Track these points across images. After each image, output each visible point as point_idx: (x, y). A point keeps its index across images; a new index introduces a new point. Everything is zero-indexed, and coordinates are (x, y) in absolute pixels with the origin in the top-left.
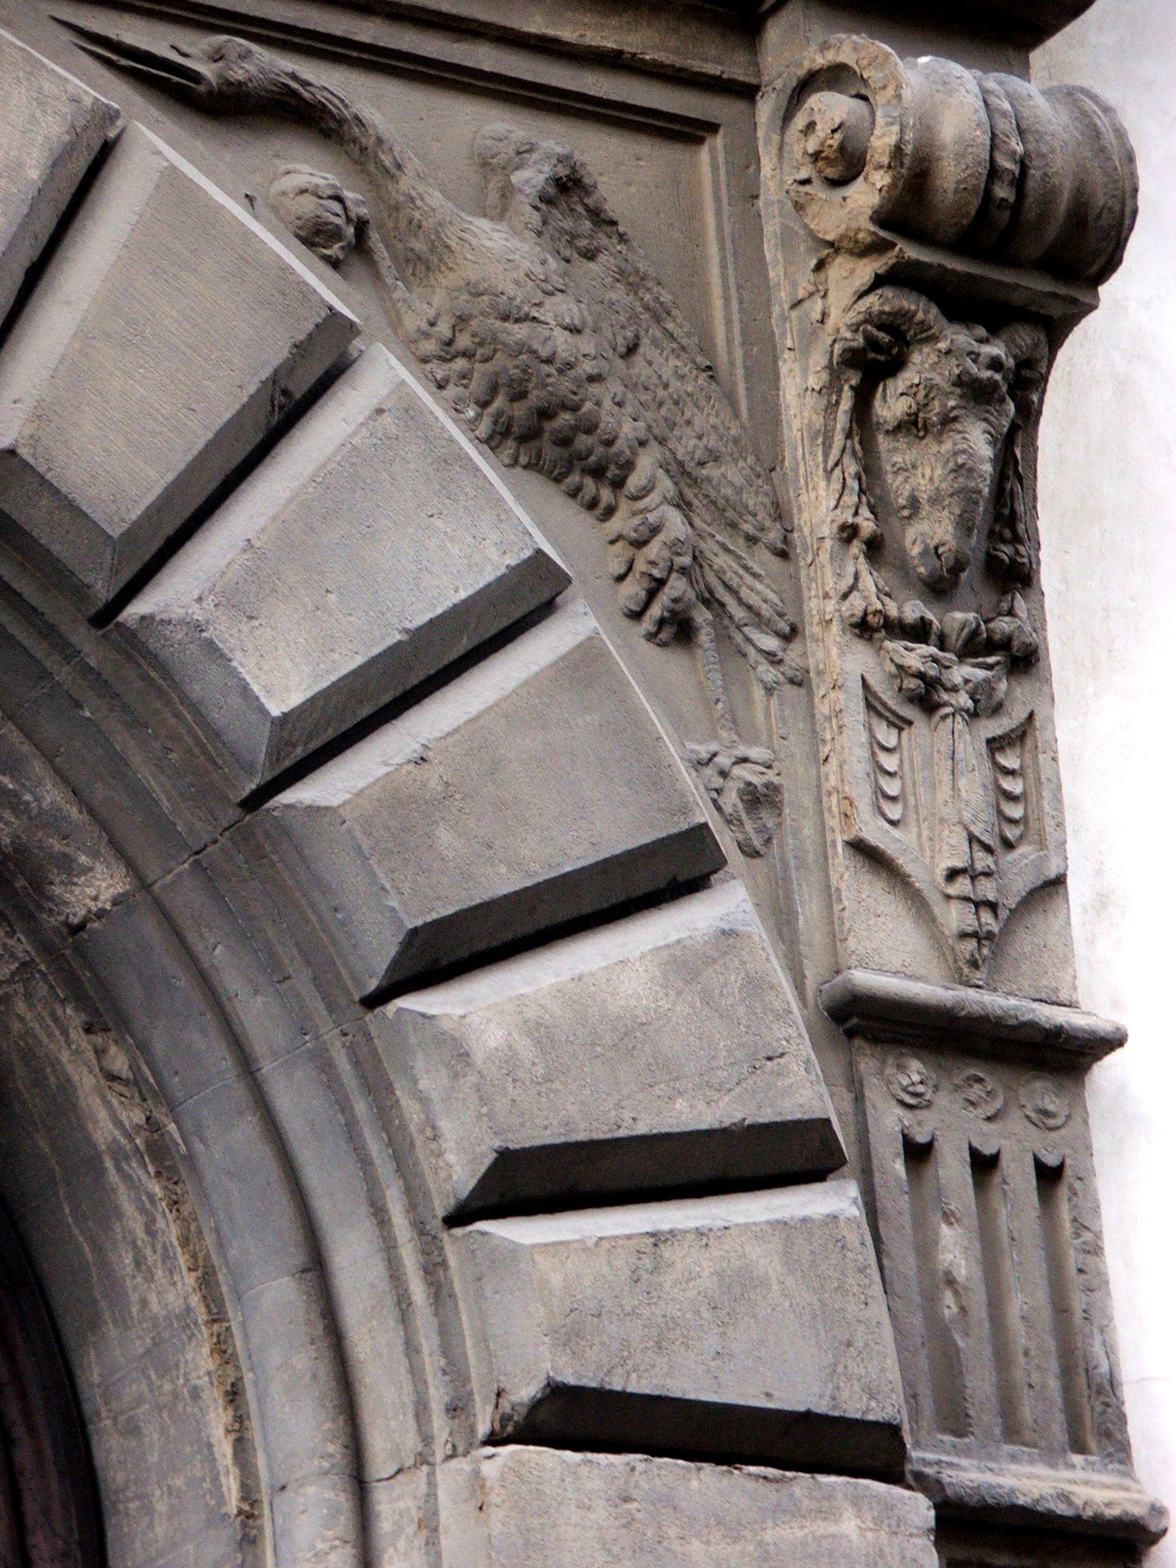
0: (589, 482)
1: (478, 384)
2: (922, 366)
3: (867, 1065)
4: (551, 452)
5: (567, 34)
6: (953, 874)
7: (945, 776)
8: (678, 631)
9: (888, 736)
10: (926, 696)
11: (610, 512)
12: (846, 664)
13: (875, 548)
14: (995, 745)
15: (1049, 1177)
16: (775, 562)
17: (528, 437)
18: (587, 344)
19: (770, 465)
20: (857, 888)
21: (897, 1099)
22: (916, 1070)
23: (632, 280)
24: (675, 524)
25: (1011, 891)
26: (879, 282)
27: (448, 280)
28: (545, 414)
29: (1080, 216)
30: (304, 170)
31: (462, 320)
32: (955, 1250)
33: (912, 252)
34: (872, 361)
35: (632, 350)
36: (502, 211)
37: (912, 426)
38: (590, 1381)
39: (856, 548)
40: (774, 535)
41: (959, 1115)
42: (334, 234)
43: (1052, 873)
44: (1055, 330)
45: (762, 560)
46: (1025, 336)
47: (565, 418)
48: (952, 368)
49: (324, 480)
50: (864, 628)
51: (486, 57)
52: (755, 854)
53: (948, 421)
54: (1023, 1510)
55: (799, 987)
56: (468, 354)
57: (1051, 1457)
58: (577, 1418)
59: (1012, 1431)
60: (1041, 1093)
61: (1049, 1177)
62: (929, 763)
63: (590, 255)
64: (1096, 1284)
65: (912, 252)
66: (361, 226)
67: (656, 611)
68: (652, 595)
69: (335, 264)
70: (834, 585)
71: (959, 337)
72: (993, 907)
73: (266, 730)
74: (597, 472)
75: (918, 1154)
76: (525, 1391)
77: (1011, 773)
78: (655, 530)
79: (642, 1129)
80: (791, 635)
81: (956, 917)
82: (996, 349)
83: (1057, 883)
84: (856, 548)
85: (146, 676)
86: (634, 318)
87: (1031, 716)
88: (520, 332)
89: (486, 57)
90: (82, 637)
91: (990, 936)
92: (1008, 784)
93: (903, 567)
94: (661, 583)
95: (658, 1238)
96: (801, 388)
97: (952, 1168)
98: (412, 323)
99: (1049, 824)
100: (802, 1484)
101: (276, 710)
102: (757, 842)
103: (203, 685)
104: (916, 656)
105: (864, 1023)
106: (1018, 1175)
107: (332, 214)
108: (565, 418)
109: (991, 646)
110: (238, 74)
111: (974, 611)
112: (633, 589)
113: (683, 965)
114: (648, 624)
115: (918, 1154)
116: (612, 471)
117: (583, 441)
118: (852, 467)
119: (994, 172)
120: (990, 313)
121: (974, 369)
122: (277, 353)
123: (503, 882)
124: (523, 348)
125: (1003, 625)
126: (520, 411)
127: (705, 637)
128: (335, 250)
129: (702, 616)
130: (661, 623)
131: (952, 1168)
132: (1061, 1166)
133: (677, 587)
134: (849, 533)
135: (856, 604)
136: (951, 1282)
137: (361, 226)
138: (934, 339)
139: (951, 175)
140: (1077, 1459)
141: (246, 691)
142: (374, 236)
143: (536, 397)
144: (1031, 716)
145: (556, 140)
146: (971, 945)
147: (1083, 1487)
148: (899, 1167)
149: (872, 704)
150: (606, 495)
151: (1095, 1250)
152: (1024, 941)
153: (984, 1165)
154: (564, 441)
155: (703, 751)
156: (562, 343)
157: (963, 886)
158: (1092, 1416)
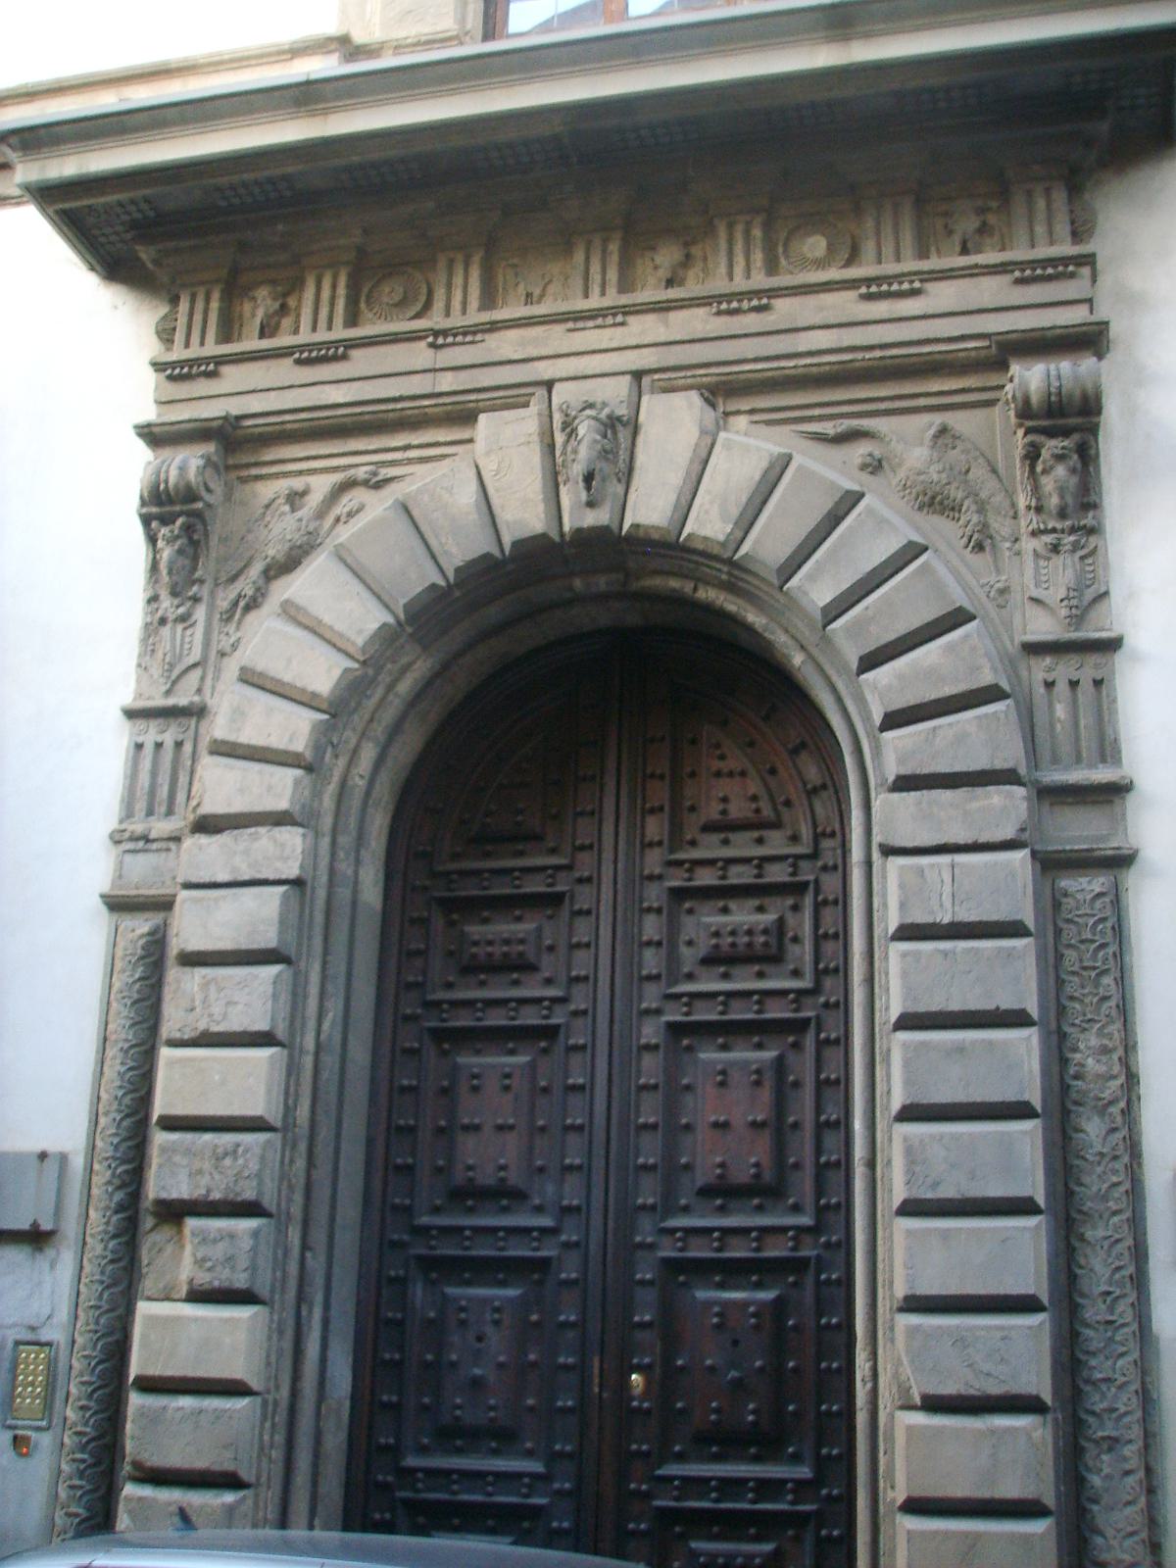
0: (951, 514)
1: (914, 495)
2: (1045, 453)
3: (1033, 662)
4: (938, 507)
5: (946, 388)
6: (1062, 601)
7: (1062, 573)
8: (980, 547)
9: (1042, 563)
10: (1055, 549)
11: (959, 519)
12: (1029, 545)
13: (1039, 509)
14: (1082, 558)
15: (1098, 683)
16: (1012, 521)
17: (931, 505)
18: (944, 475)
19: (1010, 495)
20: (1033, 611)
21: (1040, 669)
22: (1048, 660)
23: (966, 451)
24: (975, 519)
25: (1089, 597)
26: (1025, 434)
27: (904, 468)
28: (933, 498)
29: (1085, 397)
30: (860, 451)
31: (908, 478)
32: (1061, 711)
33: (1030, 423)
34: (1032, 455)
35: (968, 471)
36: (922, 444)
37: (1045, 472)
38: (909, 772)
39: (1032, 511)
40: (1011, 513)
41: (1064, 669)
42: (870, 465)
43: (1103, 589)
44: (1094, 430)
45: (1008, 521)
46: (1076, 437)
47: (939, 498)
48: (1050, 452)
49: (841, 536)
50: (1034, 534)
51: (922, 402)
52: (1003, 607)
53: (1052, 468)
54: (1072, 785)
55: (1012, 644)
56: (910, 487)
57: (1091, 766)
58: (906, 783)
59: (1078, 759)
60: (1092, 659)
61: (1098, 683)
62: (1057, 567)
63: (954, 448)
64: (1113, 712)
65: (1030, 423)
66: (880, 461)
67: (972, 544)
68: (970, 541)
69: (871, 473)
70: (1028, 521)
71: (1053, 443)
72: (1077, 607)
73: (819, 612)
74: (953, 509)
75: (1049, 685)
76: (891, 778)
77: (1090, 565)
78: (969, 522)
79: (933, 697)
80: (1016, 540)
81: (1064, 612)
82: (1065, 443)
83: (1106, 594)
84: (1032, 511)
85: (792, 602)
86: (968, 462)
87: (1096, 547)
88: (922, 477)
89: (922, 402)
90: (779, 596)
91: (1076, 616)
92: (1088, 568)
93: (1050, 513)
94: (971, 537)
95: (935, 729)
96: (1019, 472)
97: (1062, 687)
98: (894, 482)
99: (1102, 578)
100: (979, 791)
101: (822, 604)
102: (1003, 604)
103: (804, 602)
104: (1049, 539)
105: (1034, 649)
106: (1086, 685)
107: (868, 460)
108: (939, 498)
109: (1080, 528)
110: (839, 430)
111: (1079, 517)
112: (965, 539)
113: (950, 648)
114: (970, 548)
115: (1049, 685)
116: (957, 508)
117: (946, 502)
118: (1029, 488)
119: (1050, 394)
120: (1065, 433)
121: (1056, 451)
122: (829, 505)
123: (891, 636)
124: (922, 482)
125: (1082, 523)
126: (926, 499)
127: (987, 549)
128: (870, 469)
129: (987, 543)
130: (973, 548)
131: (1062, 687)
132: (1103, 680)
133: (976, 536)
134: (1029, 508)
135: (1030, 528)
136: (1059, 721)
137: (880, 461)
138: (1043, 446)
139: (1035, 399)
140: (1101, 766)
141: (813, 601)
142: (884, 463)
143: (930, 494)
144: (1096, 547)
145: (938, 419)
146: (1068, 620)
147: (1102, 775)
148: (1042, 690)
149: (1036, 554)
150: (957, 515)
151: (1114, 701)
152: (1093, 614)
153: (1074, 684)
154: (941, 503)
155: (985, 581)
156: (935, 477)
157: (1065, 603)
158: (1108, 750)
